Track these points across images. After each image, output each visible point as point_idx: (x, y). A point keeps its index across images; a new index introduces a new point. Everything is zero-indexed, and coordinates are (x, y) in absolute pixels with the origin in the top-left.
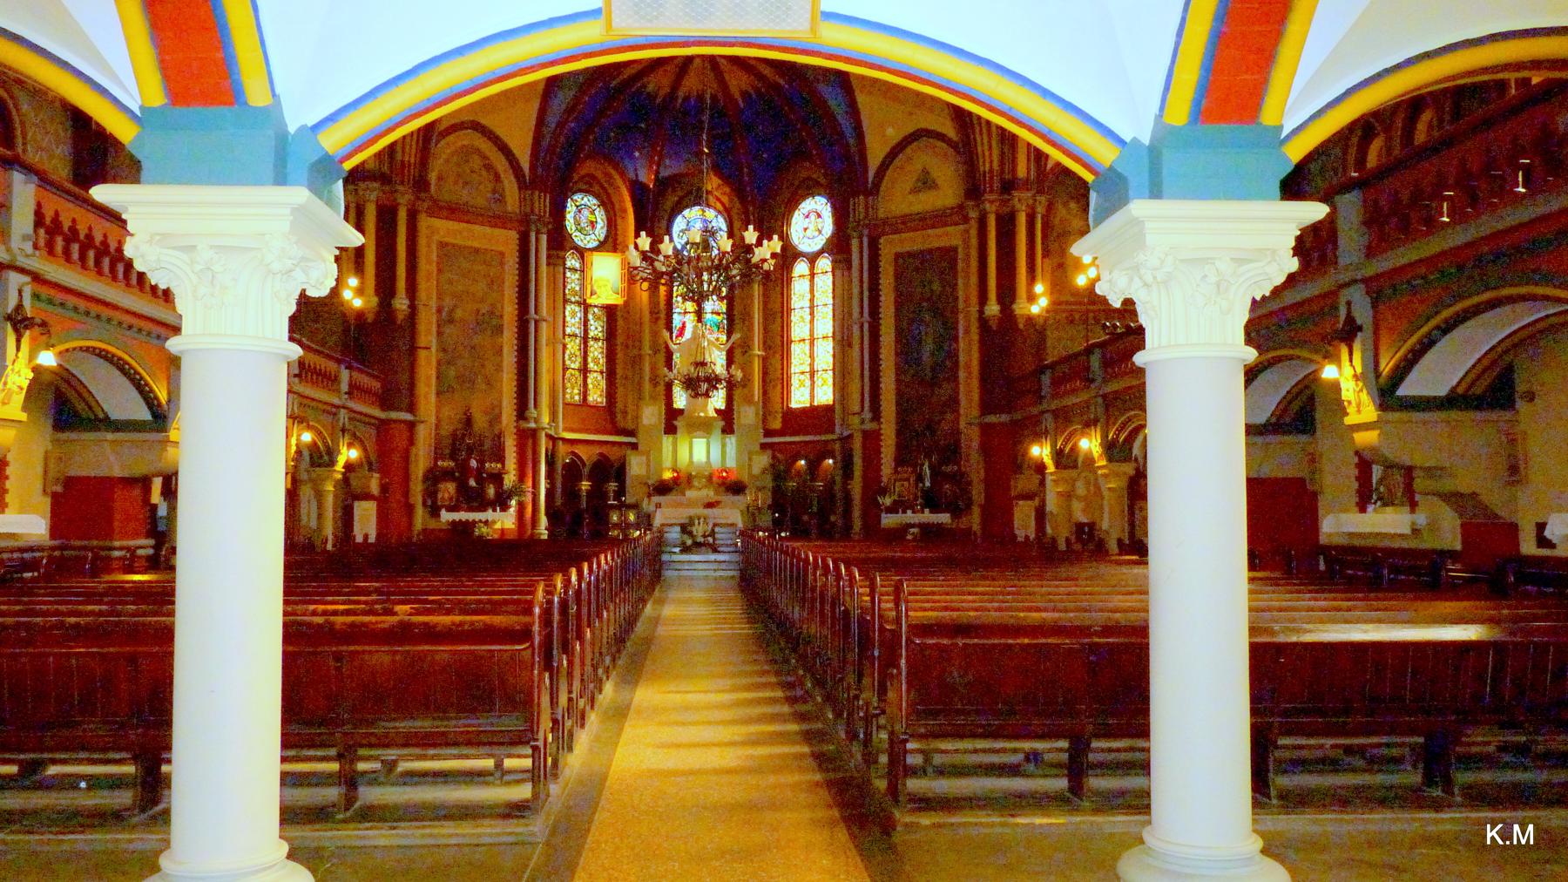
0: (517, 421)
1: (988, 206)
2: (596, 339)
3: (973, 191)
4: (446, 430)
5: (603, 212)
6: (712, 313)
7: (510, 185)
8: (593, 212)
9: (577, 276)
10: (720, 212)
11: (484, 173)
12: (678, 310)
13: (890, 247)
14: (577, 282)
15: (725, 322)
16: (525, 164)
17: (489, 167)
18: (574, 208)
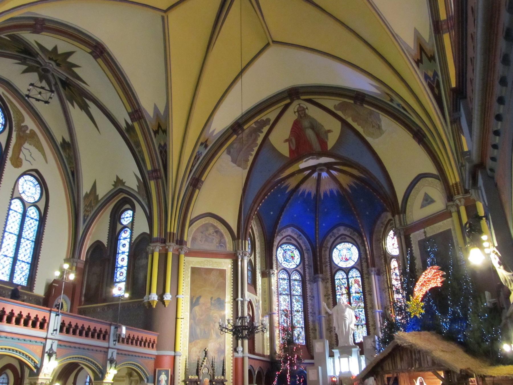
0: (233, 353)
1: (457, 202)
2: (298, 311)
3: (450, 198)
4: (195, 358)
5: (297, 252)
6: (356, 293)
7: (228, 238)
8: (292, 252)
9: (286, 282)
10: (353, 244)
11: (215, 234)
12: (339, 293)
13: (416, 237)
14: (286, 285)
15: (362, 297)
16: (235, 230)
17: (217, 232)
18: (283, 251)
